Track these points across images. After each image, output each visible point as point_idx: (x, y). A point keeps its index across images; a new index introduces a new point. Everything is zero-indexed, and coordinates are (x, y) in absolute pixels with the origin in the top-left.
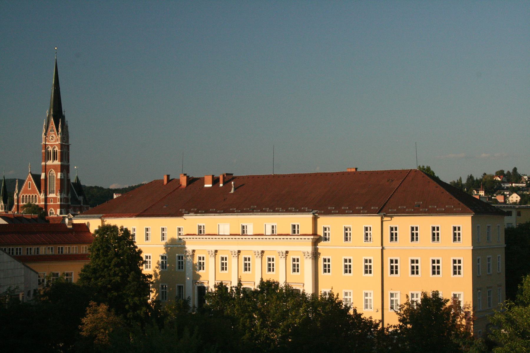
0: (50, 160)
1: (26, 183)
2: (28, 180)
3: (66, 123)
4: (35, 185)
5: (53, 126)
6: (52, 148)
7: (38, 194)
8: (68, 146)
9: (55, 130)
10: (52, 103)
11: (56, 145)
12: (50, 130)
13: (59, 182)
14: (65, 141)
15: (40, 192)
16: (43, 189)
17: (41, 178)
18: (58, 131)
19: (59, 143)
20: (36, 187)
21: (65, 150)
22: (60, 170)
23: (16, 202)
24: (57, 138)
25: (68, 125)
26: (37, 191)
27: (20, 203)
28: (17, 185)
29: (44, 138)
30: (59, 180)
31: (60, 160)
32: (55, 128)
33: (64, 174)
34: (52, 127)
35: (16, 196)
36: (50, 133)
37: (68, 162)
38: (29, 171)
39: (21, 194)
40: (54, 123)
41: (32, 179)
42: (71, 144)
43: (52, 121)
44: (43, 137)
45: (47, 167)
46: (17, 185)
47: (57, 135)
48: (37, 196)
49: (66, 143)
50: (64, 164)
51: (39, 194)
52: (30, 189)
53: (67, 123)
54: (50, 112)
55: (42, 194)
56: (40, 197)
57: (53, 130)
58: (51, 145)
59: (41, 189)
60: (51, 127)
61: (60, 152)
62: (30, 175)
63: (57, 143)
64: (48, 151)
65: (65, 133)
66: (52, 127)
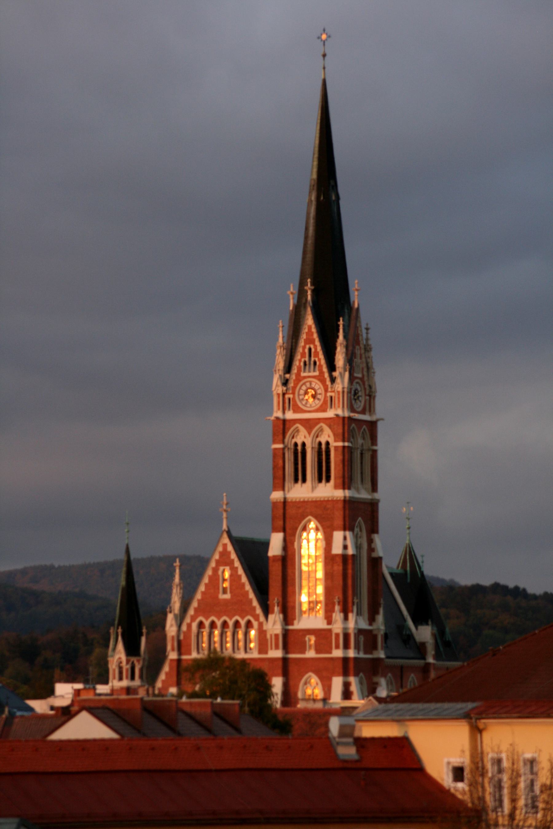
0: (304, 480)
1: (209, 572)
2: (219, 563)
3: (364, 335)
4: (244, 579)
5: (315, 347)
6: (309, 433)
7: (257, 618)
8: (372, 426)
9: (323, 362)
10: (309, 256)
11: (325, 420)
12: (302, 364)
13: (338, 568)
14: (359, 406)
15: (267, 611)
16: (275, 599)
17: (271, 553)
18: (332, 367)
19: (337, 415)
20: (248, 587)
21: (360, 441)
22: (339, 521)
23: (173, 650)
24: (329, 394)
25: (370, 342)
26: (255, 603)
27: (190, 654)
28: (177, 579)
29: (278, 394)
30: (339, 560)
31: (340, 481)
32: (321, 356)
33: (356, 537)
34: (310, 349)
35: (172, 626)
36: (303, 374)
37: (374, 488)
38: (225, 527)
39: (193, 619)
40: (315, 336)
41: (233, 556)
42: (382, 419)
43: (310, 333)
44: (275, 392)
45: (291, 511)
46: (177, 579)
47: (328, 383)
48: (255, 624)
49: (363, 412)
50: (357, 495)
51: (262, 618)
52: (228, 596)
53: (367, 333)
54: (301, 293)
55: (271, 617)
56: (265, 628)
57: (315, 363)
58: (309, 424)
59: (271, 597)
60: (307, 351)
61: (340, 450)
62: (226, 540)
63: (330, 414)
64: (296, 445)
65: (360, 375)
66: (310, 349)
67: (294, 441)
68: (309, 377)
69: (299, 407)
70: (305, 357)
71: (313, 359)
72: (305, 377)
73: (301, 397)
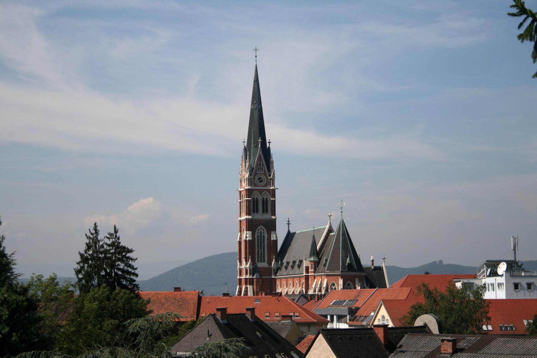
0: (257, 212)
5: (263, 163)
12: (257, 168)
34: (260, 163)
36: (257, 172)
60: (259, 164)
66: (260, 163)
67: (253, 197)
68: (261, 173)
69: (257, 185)
70: (258, 166)
71: (261, 167)
72: (258, 174)
73: (256, 181)
